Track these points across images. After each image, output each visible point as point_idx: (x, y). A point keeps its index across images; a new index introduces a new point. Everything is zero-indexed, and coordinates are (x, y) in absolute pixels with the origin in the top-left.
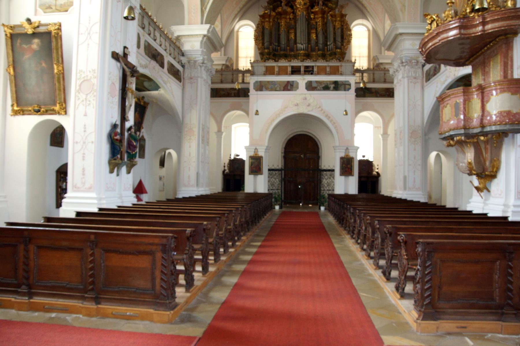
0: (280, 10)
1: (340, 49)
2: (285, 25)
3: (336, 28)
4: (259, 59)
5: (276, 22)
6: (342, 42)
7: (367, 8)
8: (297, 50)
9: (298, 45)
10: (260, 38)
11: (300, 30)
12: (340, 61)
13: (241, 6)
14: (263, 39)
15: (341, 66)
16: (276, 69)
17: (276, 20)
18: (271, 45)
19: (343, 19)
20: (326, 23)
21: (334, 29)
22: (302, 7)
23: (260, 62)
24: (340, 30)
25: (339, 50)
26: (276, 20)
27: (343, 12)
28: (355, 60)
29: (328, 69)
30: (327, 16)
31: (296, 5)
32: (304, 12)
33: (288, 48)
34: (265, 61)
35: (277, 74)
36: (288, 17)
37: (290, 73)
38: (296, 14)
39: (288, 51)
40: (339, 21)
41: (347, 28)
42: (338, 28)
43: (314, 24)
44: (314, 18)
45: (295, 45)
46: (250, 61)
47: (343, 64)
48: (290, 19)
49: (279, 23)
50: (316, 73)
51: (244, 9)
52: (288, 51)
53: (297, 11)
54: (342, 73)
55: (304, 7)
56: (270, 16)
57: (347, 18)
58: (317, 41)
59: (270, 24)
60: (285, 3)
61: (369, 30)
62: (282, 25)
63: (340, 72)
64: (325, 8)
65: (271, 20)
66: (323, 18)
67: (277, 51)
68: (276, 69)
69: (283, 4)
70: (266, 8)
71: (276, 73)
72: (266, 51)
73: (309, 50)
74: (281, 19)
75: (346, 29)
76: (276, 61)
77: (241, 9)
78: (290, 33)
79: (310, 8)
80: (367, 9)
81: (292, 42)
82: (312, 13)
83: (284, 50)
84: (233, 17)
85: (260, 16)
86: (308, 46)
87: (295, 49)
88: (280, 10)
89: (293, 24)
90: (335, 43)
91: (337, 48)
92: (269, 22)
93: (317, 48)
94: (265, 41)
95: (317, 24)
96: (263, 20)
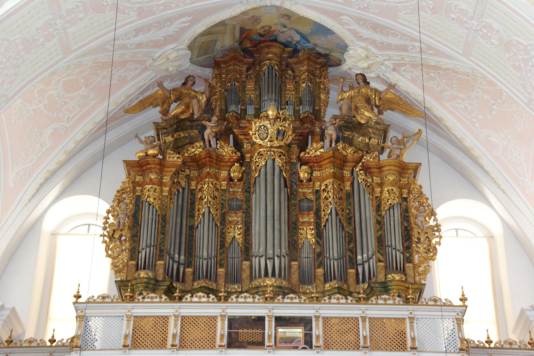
0: (197, 149)
1: (403, 271)
2: (215, 198)
3: (385, 207)
4: (115, 292)
5: (184, 189)
6: (407, 248)
7: (483, 161)
8: (251, 278)
9: (255, 261)
10: (126, 234)
11: (263, 214)
12: (407, 301)
13: (71, 146)
14: (135, 237)
15: (412, 319)
16: (173, 328)
17: (183, 184)
18: (161, 257)
19: (404, 181)
20: (350, 195)
21: (378, 208)
22: (269, 144)
23: (112, 302)
24: (397, 212)
25: (397, 277)
26: (183, 184)
27: (408, 158)
28: (463, 299)
29: (364, 331)
30: (352, 172)
31: (249, 140)
32: (278, 160)
33: (221, 271)
34: (132, 299)
35: (172, 346)
36: (224, 174)
37: (225, 342)
38: (250, 167)
39: (221, 281)
40: (394, 183)
41: (421, 204)
42: (392, 207)
43: (311, 197)
44: (310, 180)
45: (246, 263)
46: (78, 297)
47: (418, 311)
48: (231, 179)
49: (192, 193)
50: (321, 343)
51: (80, 159)
52: (221, 281)
53: (251, 157)
54: (417, 345)
55: (276, 143)
56: (162, 165)
57: (422, 179)
58: (318, 250)
59: (162, 191)
60: (217, 130)
61: (491, 238)
62: (201, 199)
63: (409, 344)
64: (343, 149)
65: (167, 179)
66: (339, 178)
67: (183, 281)
68: (173, 328)
69: (207, 133)
70: (149, 142)
71: (170, 342)
72: (143, 274)
73: (295, 277)
74: (200, 179)
75: (417, 209)
76: (172, 299)
77: (72, 156)
78: (230, 222)
79: (295, 148)
80: (481, 166)
81: (235, 253)
82: (304, 162)
83: (208, 277)
84: (40, 180)
85: (128, 164)
86: (290, 267)
87: (245, 275)
88: (197, 149)
89: (240, 196)
90: (384, 255)
91: (388, 269)
92: (161, 184)
93: (320, 271)
94: (143, 244)
95: (318, 198)
96: (138, 179)
